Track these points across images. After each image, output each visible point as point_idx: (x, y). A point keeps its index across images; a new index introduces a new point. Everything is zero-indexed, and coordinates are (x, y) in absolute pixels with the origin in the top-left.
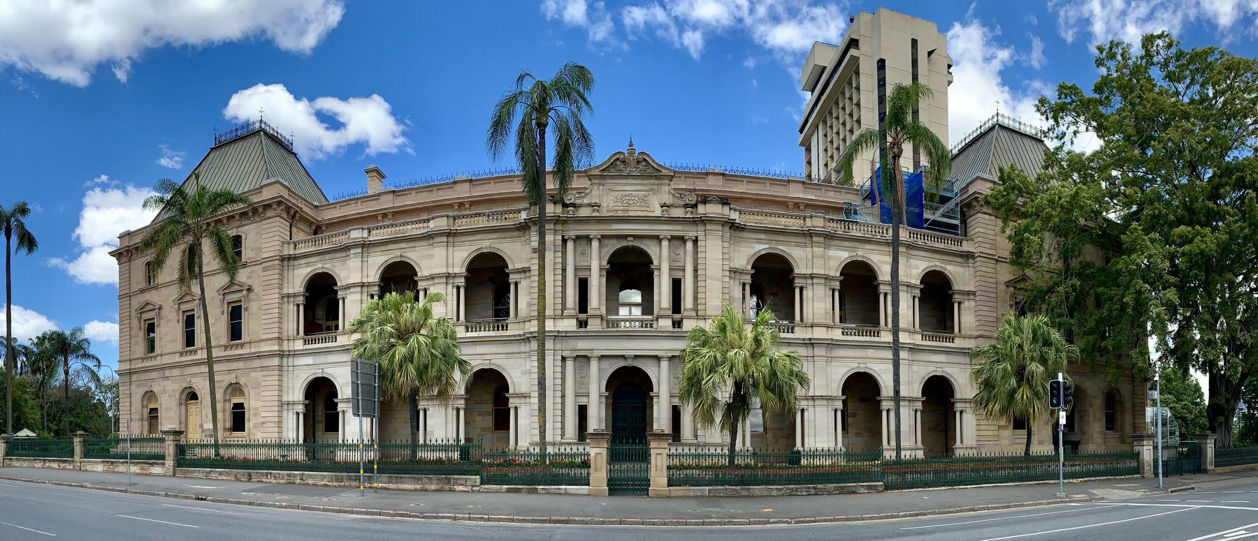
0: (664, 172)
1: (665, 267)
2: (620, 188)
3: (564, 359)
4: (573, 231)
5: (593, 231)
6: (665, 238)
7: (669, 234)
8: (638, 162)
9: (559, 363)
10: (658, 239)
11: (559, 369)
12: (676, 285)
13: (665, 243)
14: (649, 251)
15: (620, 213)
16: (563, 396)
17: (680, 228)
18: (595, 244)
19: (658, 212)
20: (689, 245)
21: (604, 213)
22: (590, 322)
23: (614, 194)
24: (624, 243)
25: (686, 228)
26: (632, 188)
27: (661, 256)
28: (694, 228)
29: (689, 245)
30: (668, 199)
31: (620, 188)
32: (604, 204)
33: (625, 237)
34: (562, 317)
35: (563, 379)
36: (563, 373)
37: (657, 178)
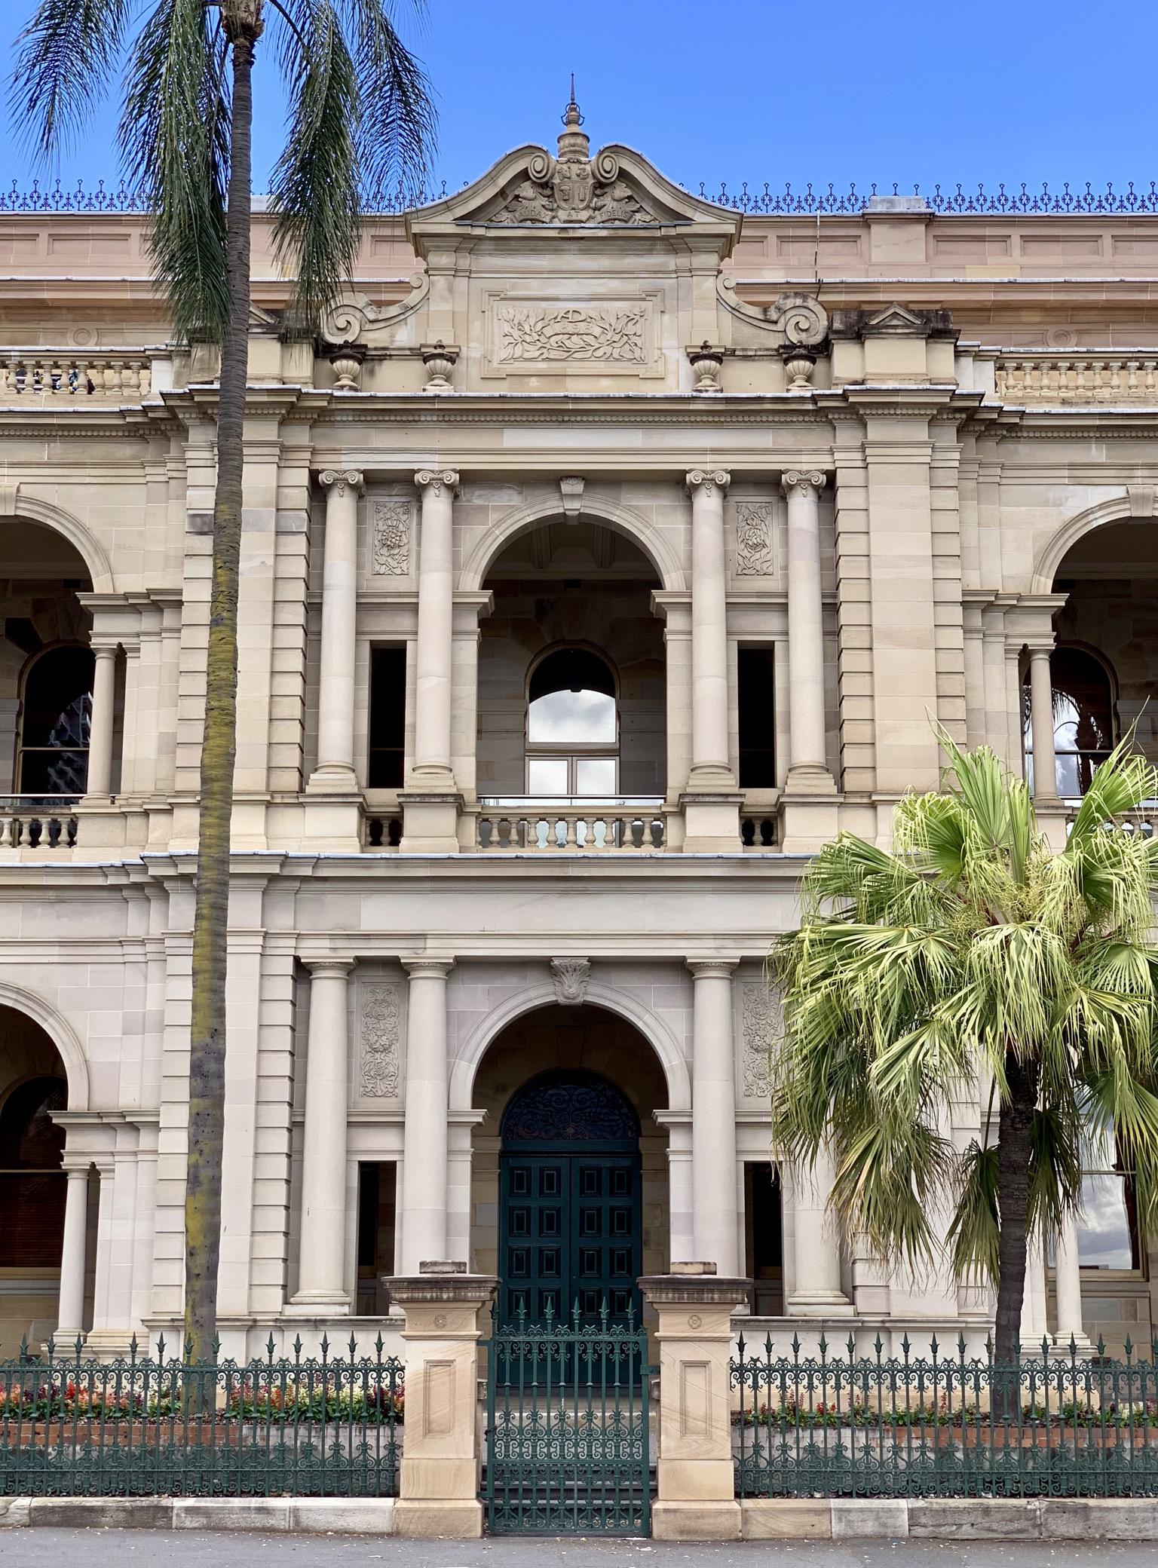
0: (703, 222)
1: (709, 599)
2: (534, 287)
3: (303, 972)
4: (355, 453)
5: (431, 454)
6: (710, 481)
7: (721, 468)
8: (601, 186)
9: (284, 988)
10: (678, 484)
11: (283, 1014)
12: (755, 668)
13: (708, 502)
14: (646, 536)
15: (535, 389)
16: (296, 1127)
17: (762, 439)
18: (437, 506)
19: (677, 380)
20: (803, 508)
21: (471, 385)
22: (412, 821)
23: (509, 310)
24: (548, 506)
25: (787, 438)
26: (579, 288)
27: (691, 553)
28: (818, 438)
29: (803, 508)
30: (720, 331)
31: (534, 287)
32: (472, 351)
33: (552, 480)
34: (301, 798)
35: (299, 1053)
36: (300, 1026)
37: (675, 245)
